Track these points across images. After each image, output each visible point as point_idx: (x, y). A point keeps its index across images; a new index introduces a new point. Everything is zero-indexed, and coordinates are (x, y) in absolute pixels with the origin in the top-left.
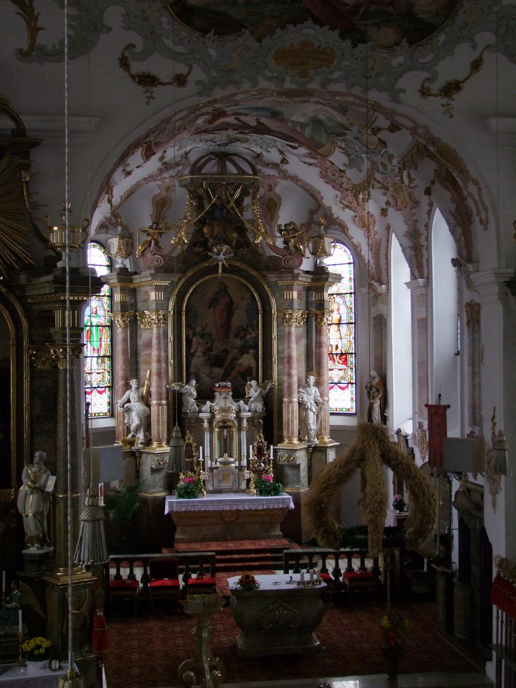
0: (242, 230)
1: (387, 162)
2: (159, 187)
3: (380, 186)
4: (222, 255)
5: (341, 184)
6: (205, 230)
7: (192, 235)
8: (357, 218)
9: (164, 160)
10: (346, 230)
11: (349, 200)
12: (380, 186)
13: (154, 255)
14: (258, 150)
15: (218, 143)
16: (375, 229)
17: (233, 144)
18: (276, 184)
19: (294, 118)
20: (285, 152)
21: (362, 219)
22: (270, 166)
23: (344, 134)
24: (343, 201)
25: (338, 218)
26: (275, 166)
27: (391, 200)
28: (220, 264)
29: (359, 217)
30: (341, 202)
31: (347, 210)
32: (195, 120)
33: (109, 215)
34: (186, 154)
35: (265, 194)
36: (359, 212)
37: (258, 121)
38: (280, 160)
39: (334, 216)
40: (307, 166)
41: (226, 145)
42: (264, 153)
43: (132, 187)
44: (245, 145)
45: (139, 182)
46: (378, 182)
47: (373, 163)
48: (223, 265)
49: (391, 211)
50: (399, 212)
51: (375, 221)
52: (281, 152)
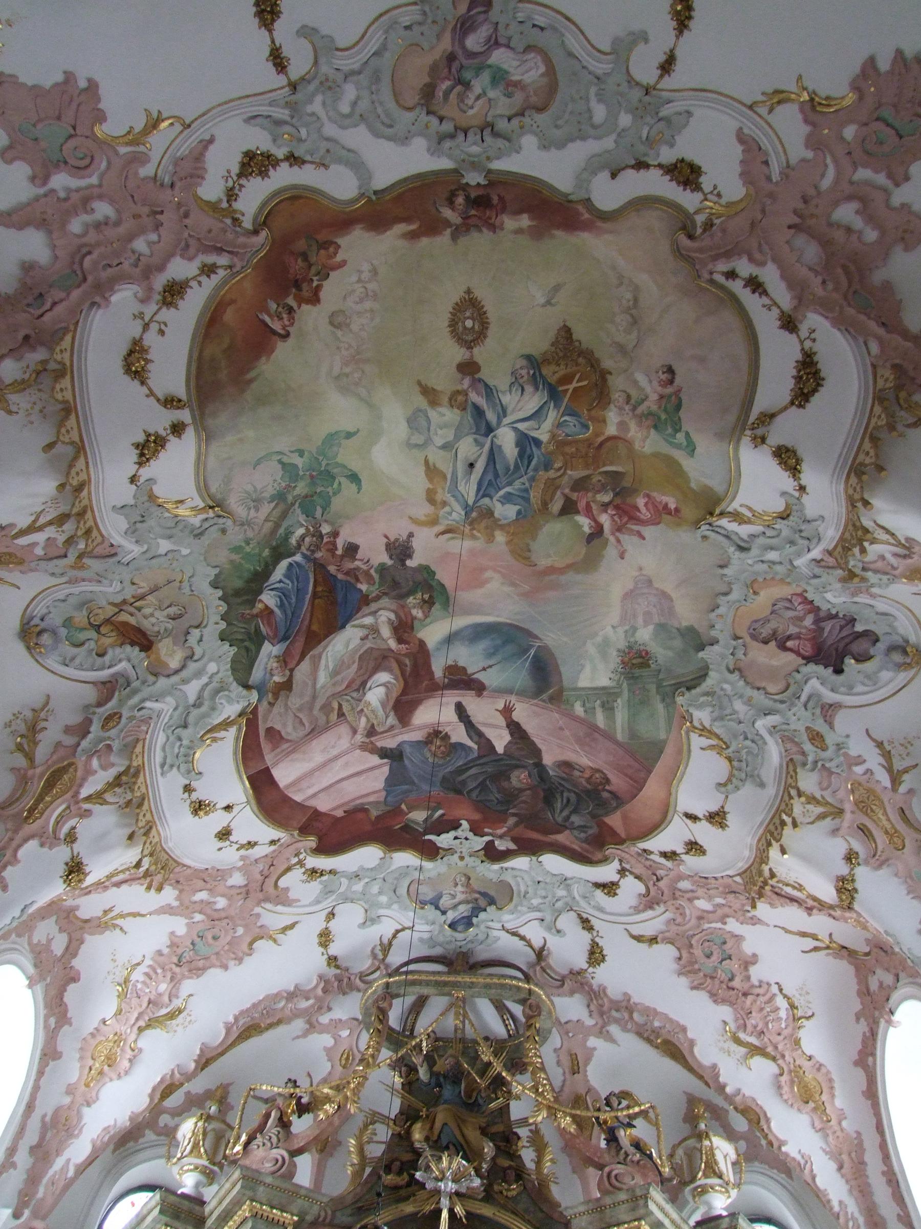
0: (506, 1141)
1: (820, 726)
2: (329, 1051)
3: (820, 810)
4: (448, 1177)
5: (731, 980)
6: (417, 1135)
7: (383, 1147)
8: (784, 1079)
9: (333, 950)
10: (763, 1122)
11: (755, 1027)
12: (820, 810)
13: (271, 1148)
14: (536, 934)
15: (451, 916)
16: (838, 1103)
17: (482, 915)
18: (590, 1053)
19: (584, 682)
20: (594, 922)
21: (796, 1074)
22: (568, 984)
23: (702, 675)
24: (742, 1036)
25: (738, 1092)
26: (576, 981)
27: (857, 846)
28: (445, 1203)
29: (790, 1072)
30: (738, 1041)
31: (758, 1062)
32: (362, 686)
33: (193, 1065)
34: (386, 948)
35: (564, 1081)
36: (787, 1054)
37: (507, 711)
38: (585, 933)
39: (728, 1090)
40: (644, 946)
41: (468, 922)
42: (554, 942)
43: (254, 1006)
44: (509, 919)
45: (276, 997)
46: (812, 800)
47: (787, 738)
48: (451, 1211)
49: (863, 874)
50: (884, 872)
51: (831, 1080)
52: (586, 924)
